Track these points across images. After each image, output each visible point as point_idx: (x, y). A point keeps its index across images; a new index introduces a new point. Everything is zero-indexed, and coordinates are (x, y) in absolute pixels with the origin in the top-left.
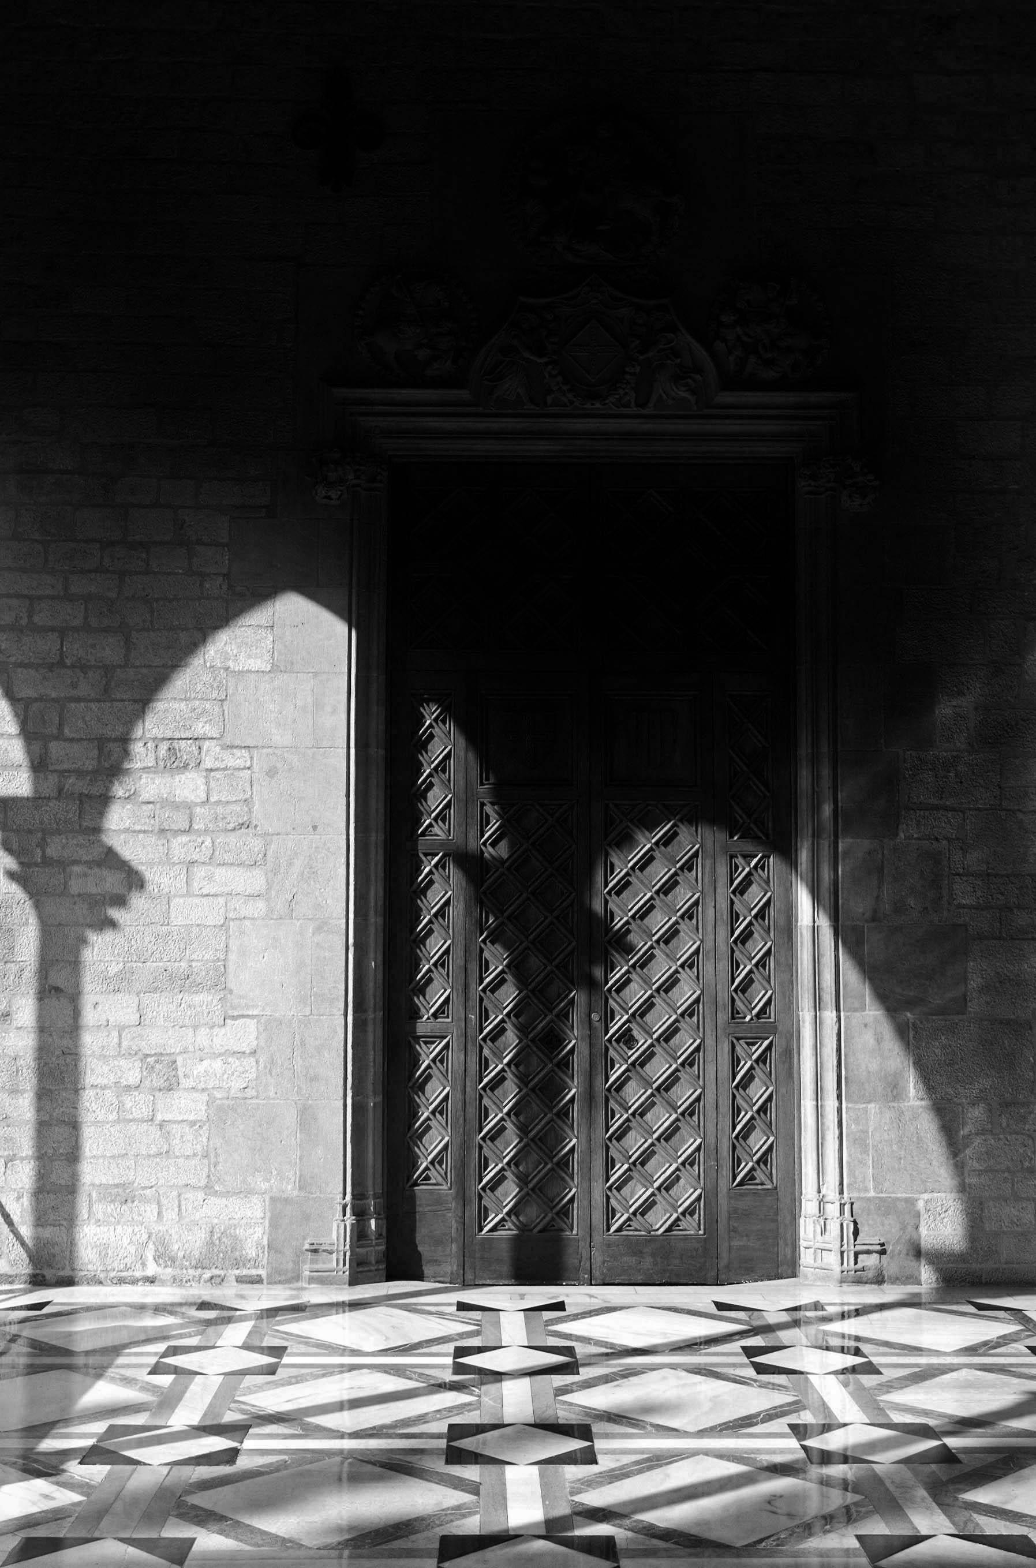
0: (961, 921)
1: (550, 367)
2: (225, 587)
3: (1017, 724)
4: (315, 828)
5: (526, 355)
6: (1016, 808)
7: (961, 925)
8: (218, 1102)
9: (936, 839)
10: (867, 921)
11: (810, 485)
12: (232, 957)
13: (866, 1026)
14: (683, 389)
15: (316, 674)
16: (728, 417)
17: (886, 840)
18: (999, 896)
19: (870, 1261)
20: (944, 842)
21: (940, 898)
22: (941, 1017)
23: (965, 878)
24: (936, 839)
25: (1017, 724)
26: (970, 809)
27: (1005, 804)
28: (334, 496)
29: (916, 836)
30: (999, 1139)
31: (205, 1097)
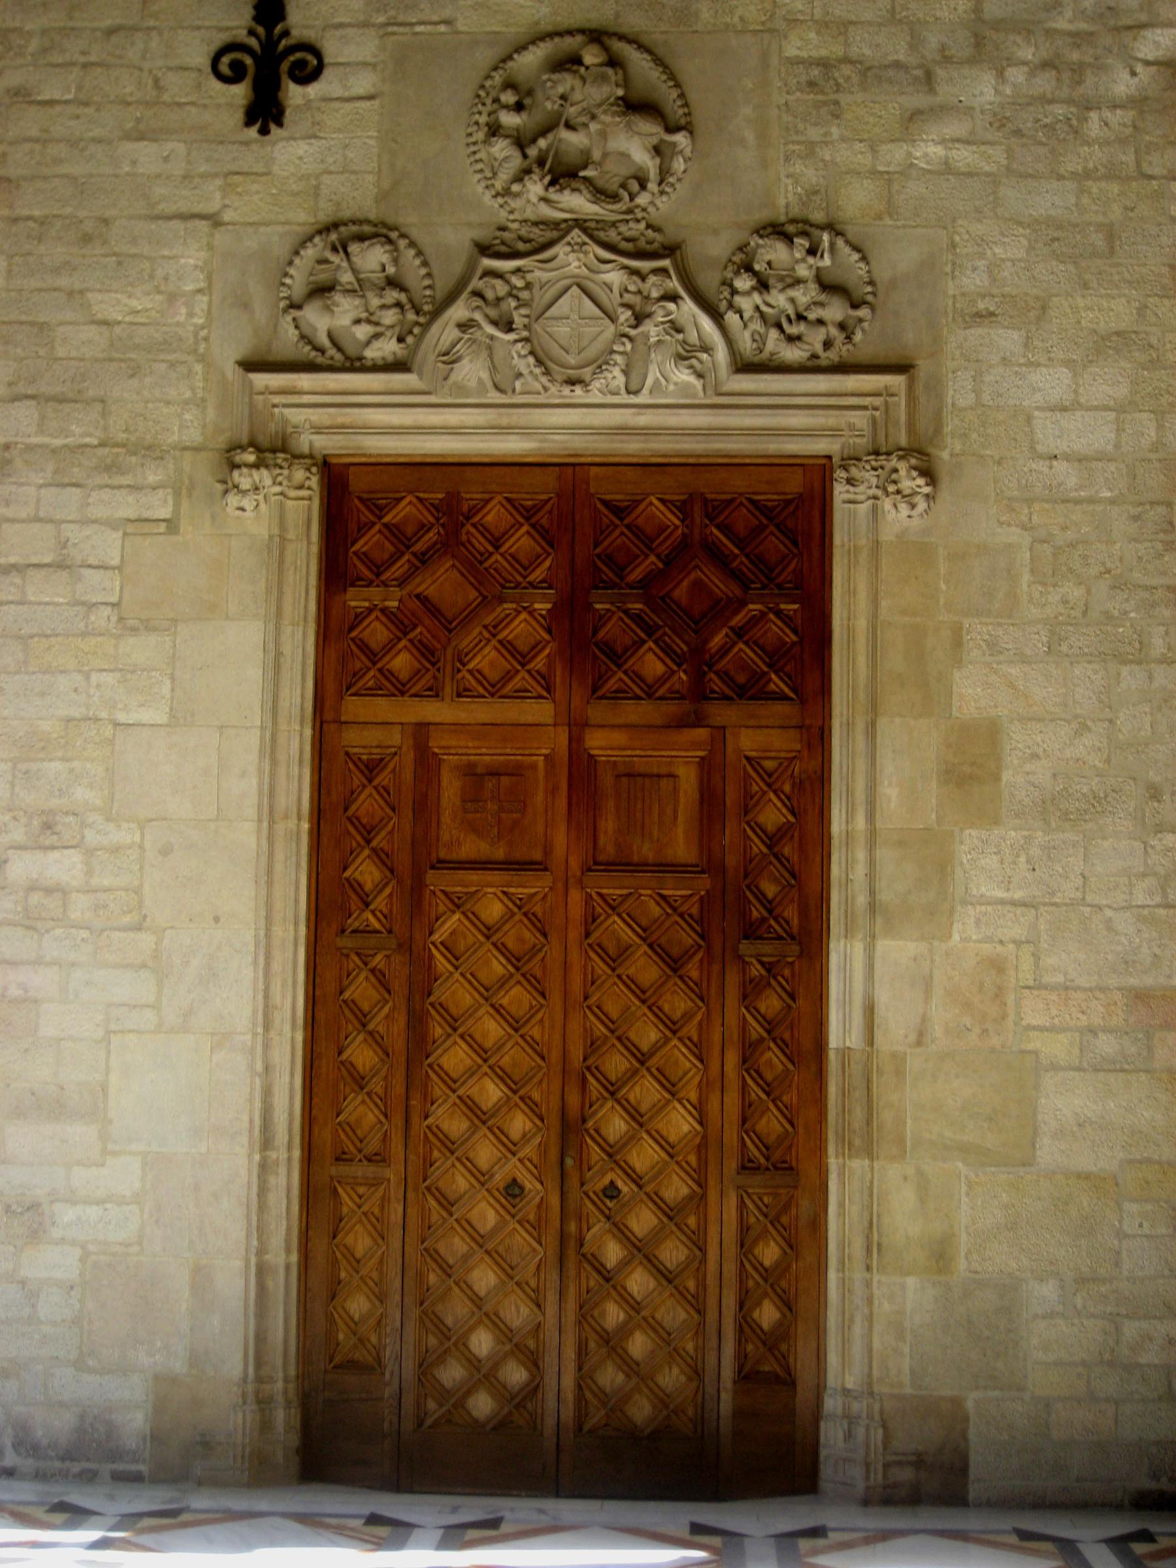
0: (1030, 1047)
1: (520, 345)
2: (114, 619)
3: (1106, 797)
4: (217, 920)
5: (490, 330)
6: (1104, 902)
7: (1030, 1052)
8: (93, 1257)
9: (1001, 942)
10: (910, 1046)
11: (848, 492)
12: (114, 1078)
13: (905, 1178)
14: (687, 371)
15: (221, 727)
16: (737, 407)
17: (936, 943)
18: (1080, 1016)
19: (905, 1475)
20: (1011, 946)
21: (1004, 1017)
22: (1003, 1169)
23: (1035, 992)
24: (1001, 942)
25: (1106, 797)
26: (1045, 904)
27: (1089, 899)
28: (247, 507)
29: (974, 937)
30: (1073, 1325)
31: (78, 1252)
